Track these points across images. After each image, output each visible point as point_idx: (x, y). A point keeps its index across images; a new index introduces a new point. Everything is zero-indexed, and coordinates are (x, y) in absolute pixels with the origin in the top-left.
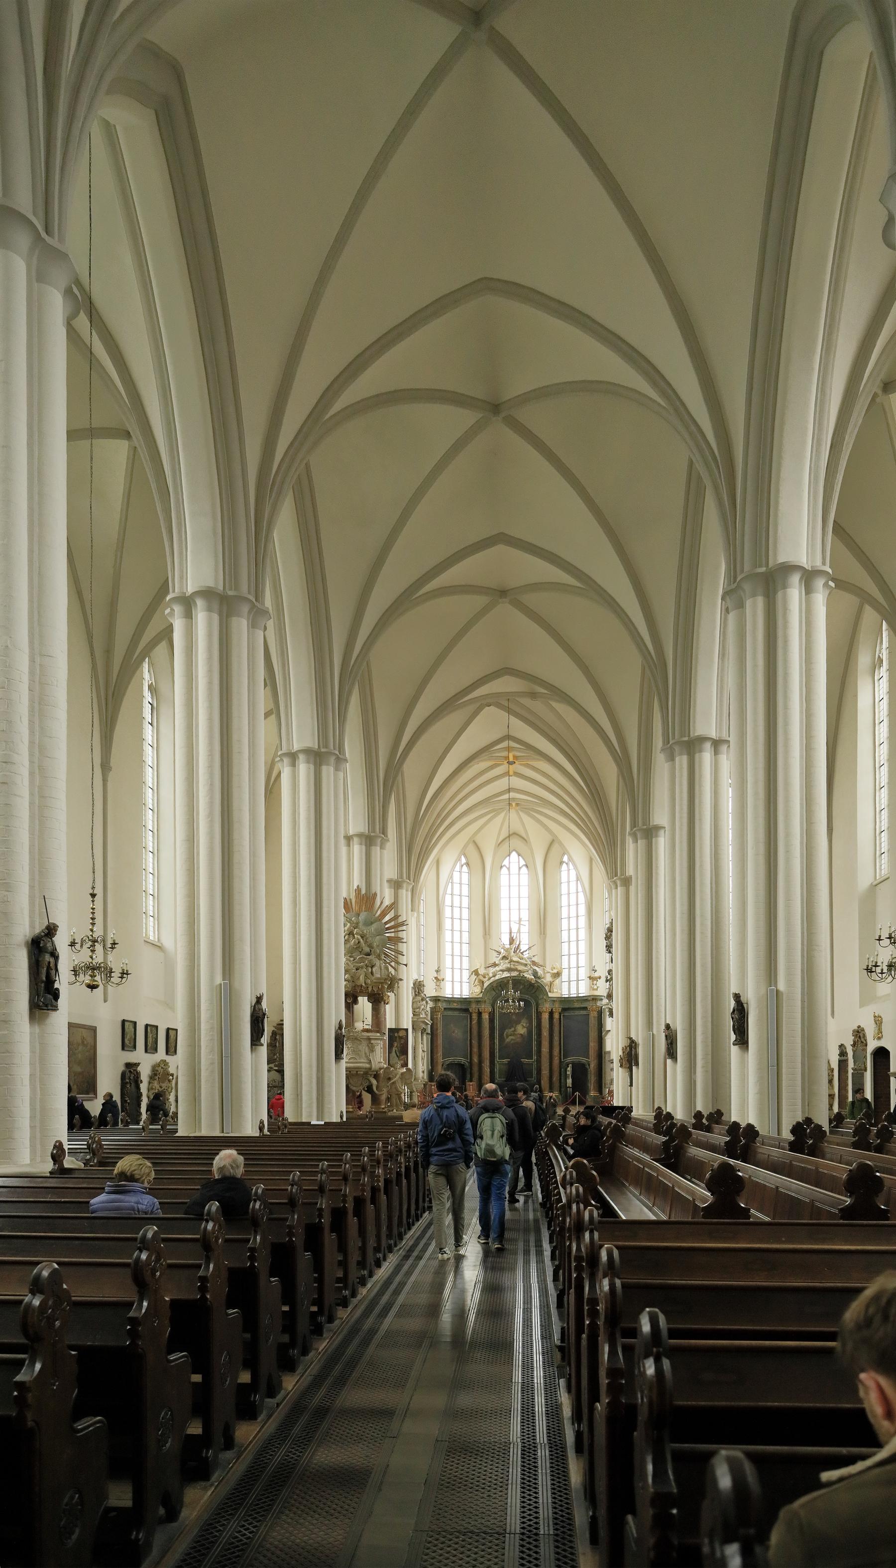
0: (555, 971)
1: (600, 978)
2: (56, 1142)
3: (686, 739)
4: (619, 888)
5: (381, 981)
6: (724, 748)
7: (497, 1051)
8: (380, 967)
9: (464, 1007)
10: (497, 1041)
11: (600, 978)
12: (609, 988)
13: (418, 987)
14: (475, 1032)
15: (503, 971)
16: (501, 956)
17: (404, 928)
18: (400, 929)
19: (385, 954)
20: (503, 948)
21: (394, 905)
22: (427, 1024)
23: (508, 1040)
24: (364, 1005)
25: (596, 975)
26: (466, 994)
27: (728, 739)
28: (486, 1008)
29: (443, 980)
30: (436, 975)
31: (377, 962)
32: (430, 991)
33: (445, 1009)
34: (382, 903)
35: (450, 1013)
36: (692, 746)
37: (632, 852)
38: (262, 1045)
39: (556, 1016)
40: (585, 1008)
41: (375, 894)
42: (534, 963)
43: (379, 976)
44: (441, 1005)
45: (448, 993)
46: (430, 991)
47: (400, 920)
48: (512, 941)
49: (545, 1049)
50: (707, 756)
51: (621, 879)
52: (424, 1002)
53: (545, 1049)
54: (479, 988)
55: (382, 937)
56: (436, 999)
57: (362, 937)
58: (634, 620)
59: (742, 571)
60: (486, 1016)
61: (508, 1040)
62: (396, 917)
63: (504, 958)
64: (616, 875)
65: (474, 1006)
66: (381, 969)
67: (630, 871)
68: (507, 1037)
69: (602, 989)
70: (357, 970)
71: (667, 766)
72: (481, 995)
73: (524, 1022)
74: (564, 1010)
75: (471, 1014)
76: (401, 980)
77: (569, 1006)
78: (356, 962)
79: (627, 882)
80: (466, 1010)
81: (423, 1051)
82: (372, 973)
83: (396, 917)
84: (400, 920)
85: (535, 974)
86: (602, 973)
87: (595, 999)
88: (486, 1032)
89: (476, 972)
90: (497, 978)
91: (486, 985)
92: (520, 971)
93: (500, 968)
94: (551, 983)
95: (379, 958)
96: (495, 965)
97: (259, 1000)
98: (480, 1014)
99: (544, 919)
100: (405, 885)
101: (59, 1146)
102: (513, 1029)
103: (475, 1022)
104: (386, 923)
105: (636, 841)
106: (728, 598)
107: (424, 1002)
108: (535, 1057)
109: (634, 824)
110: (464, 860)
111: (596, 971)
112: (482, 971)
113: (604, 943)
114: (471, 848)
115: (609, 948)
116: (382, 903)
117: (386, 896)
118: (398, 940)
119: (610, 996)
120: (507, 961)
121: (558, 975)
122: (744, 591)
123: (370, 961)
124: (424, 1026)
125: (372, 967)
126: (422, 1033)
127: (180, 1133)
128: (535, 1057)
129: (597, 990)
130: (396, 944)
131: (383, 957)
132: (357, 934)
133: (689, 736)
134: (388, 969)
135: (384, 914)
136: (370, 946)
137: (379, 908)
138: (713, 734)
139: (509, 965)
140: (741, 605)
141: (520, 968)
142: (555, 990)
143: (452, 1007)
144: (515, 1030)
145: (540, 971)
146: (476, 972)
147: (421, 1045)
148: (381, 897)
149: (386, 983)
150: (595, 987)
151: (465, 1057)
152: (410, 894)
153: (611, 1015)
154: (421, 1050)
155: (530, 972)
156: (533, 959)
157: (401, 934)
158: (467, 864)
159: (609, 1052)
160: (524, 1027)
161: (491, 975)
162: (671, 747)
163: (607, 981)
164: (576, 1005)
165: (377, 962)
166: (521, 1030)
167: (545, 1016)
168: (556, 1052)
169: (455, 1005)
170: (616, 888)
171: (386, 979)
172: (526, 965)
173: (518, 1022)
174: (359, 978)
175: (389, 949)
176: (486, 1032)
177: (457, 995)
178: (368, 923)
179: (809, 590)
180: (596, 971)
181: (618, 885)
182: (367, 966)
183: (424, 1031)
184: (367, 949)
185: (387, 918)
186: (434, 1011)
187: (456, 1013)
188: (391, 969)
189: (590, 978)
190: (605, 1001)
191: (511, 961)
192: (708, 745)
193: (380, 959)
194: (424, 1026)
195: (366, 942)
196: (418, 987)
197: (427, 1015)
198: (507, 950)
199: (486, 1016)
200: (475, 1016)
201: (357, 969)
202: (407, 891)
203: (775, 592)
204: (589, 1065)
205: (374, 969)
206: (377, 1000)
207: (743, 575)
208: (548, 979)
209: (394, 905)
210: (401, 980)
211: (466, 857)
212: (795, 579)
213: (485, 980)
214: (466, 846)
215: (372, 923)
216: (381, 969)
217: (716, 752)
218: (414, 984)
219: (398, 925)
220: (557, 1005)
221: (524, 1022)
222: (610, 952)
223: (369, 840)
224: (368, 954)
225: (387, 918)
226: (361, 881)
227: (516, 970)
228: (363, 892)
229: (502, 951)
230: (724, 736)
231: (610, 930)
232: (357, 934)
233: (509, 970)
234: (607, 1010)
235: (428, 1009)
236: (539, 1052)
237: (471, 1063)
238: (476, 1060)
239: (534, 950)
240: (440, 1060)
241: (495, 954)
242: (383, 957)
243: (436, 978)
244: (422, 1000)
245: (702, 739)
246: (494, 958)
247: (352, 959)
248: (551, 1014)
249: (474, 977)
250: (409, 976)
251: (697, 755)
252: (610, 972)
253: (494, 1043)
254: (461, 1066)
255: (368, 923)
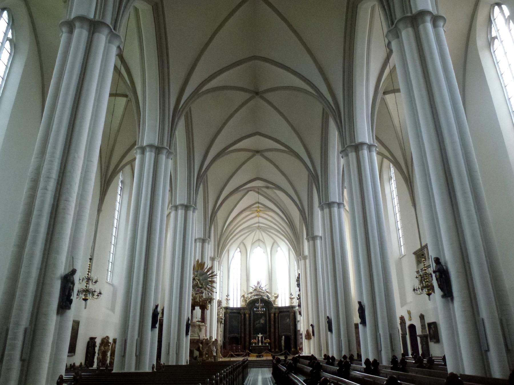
0: (276, 295)
1: (294, 298)
2: (61, 375)
3: (328, 202)
4: (302, 260)
5: (206, 300)
6: (342, 206)
7: (252, 331)
8: (206, 293)
9: (237, 311)
10: (252, 326)
11: (294, 298)
12: (299, 302)
13: (220, 303)
14: (243, 323)
15: (254, 296)
16: (253, 289)
17: (215, 277)
18: (213, 277)
19: (208, 288)
20: (254, 286)
21: (211, 268)
22: (222, 319)
23: (257, 326)
24: (198, 310)
25: (293, 297)
26: (239, 306)
27: (342, 203)
28: (247, 312)
29: (229, 300)
30: (226, 298)
31: (204, 291)
32: (224, 305)
33: (230, 312)
34: (207, 266)
35: (233, 314)
36: (330, 205)
37: (306, 246)
38: (156, 328)
39: (277, 315)
40: (288, 311)
41: (205, 263)
42: (267, 292)
43: (205, 297)
44: (229, 311)
45: (231, 305)
46: (224, 305)
47: (213, 274)
48: (258, 283)
49: (272, 330)
50: (335, 209)
51: (302, 257)
52: (222, 309)
53: (272, 330)
54: (245, 303)
55: (206, 281)
56: (227, 308)
57: (199, 281)
58: (306, 162)
59: (346, 144)
60: (247, 316)
61: (257, 326)
62: (212, 273)
63: (255, 290)
64: (300, 255)
65: (242, 311)
66: (206, 294)
67: (306, 253)
68: (256, 324)
69: (295, 303)
70: (196, 294)
71: (320, 212)
72: (245, 306)
73: (263, 318)
74: (280, 312)
75: (241, 314)
76: (214, 299)
77: (283, 311)
78: (196, 291)
79: (305, 258)
80: (239, 313)
81: (221, 331)
82: (202, 296)
83: (212, 273)
84: (213, 274)
85: (268, 296)
86: (295, 295)
87: (292, 307)
88: (247, 323)
89: (243, 296)
90: (252, 299)
91: (248, 301)
92: (261, 296)
93: (253, 294)
94: (274, 301)
95: (205, 289)
96: (251, 293)
97: (157, 307)
98: (245, 315)
99: (271, 273)
100: (216, 259)
101: (61, 377)
102: (259, 321)
103: (242, 318)
104: (209, 275)
105: (308, 241)
106: (342, 153)
107: (222, 309)
108: (268, 334)
109: (307, 235)
110: (239, 250)
111: (292, 295)
112: (246, 296)
113: (296, 283)
114: (242, 245)
115: (298, 285)
116: (207, 266)
117: (208, 264)
118: (213, 282)
119: (299, 306)
120: (256, 291)
121: (277, 297)
122: (348, 151)
123: (202, 291)
124: (221, 320)
125: (202, 293)
126: (220, 323)
127: (114, 371)
128: (268, 334)
129: (293, 303)
130: (212, 284)
131: (207, 289)
132: (197, 279)
133: (329, 201)
134: (209, 294)
135: (208, 271)
136: (202, 285)
137: (206, 268)
138: (338, 201)
139: (257, 293)
140: (347, 155)
141: (262, 294)
142: (276, 304)
143: (232, 311)
144: (260, 322)
145: (270, 296)
146: (243, 296)
147: (220, 329)
148: (207, 263)
149: (208, 301)
150: (292, 302)
151: (239, 334)
152: (218, 262)
153: (300, 314)
154: (220, 331)
155: (266, 296)
156: (267, 290)
157: (215, 280)
158: (240, 251)
159: (299, 331)
160: (263, 320)
161: (249, 297)
162: (322, 206)
163: (298, 299)
164: (285, 310)
165: (204, 291)
166: (262, 321)
167: (272, 315)
168: (277, 331)
169: (235, 311)
170: (301, 260)
171: (208, 299)
172: (264, 293)
173: (261, 318)
174: (196, 298)
175: (209, 286)
176: (247, 323)
177: (235, 306)
178: (201, 275)
179: (370, 151)
180: (292, 295)
181: (302, 259)
182: (200, 293)
183: (221, 322)
184: (200, 286)
185: (208, 273)
186: (225, 314)
187: (235, 314)
188: (210, 294)
189: (290, 298)
190: (298, 308)
191: (258, 291)
192: (336, 205)
193: (206, 290)
194: (221, 320)
195: (200, 282)
196: (220, 303)
197: (222, 315)
198: (256, 287)
199: (247, 316)
200: (243, 315)
201: (196, 294)
202: (217, 262)
203: (359, 151)
204: (291, 336)
205: (203, 294)
206: (203, 308)
207: (347, 146)
208: (272, 299)
209: (211, 268)
210: (214, 299)
211: (239, 248)
212: (365, 147)
213: (247, 299)
214: (240, 244)
215: (203, 275)
216: (206, 294)
217: (339, 208)
218: (218, 302)
219: (213, 275)
220: (277, 310)
221: (263, 318)
222: (298, 287)
223: (203, 241)
224: (201, 288)
225: (208, 273)
226: (199, 257)
227: (260, 295)
228: (200, 262)
229: (254, 287)
230: (341, 201)
231: (299, 278)
232: (197, 279)
233: (257, 295)
234: (298, 312)
235: (223, 313)
236: (270, 331)
237: (241, 337)
238: (243, 335)
239: (267, 287)
240: (228, 335)
241: (251, 288)
242: (207, 289)
243: (227, 299)
244: (221, 308)
245: (334, 203)
246: (251, 290)
247: (194, 290)
248: (275, 314)
249: (242, 298)
250: (217, 297)
251: (332, 209)
252: (299, 295)
253: (251, 327)
254: (236, 338)
255: (201, 275)
